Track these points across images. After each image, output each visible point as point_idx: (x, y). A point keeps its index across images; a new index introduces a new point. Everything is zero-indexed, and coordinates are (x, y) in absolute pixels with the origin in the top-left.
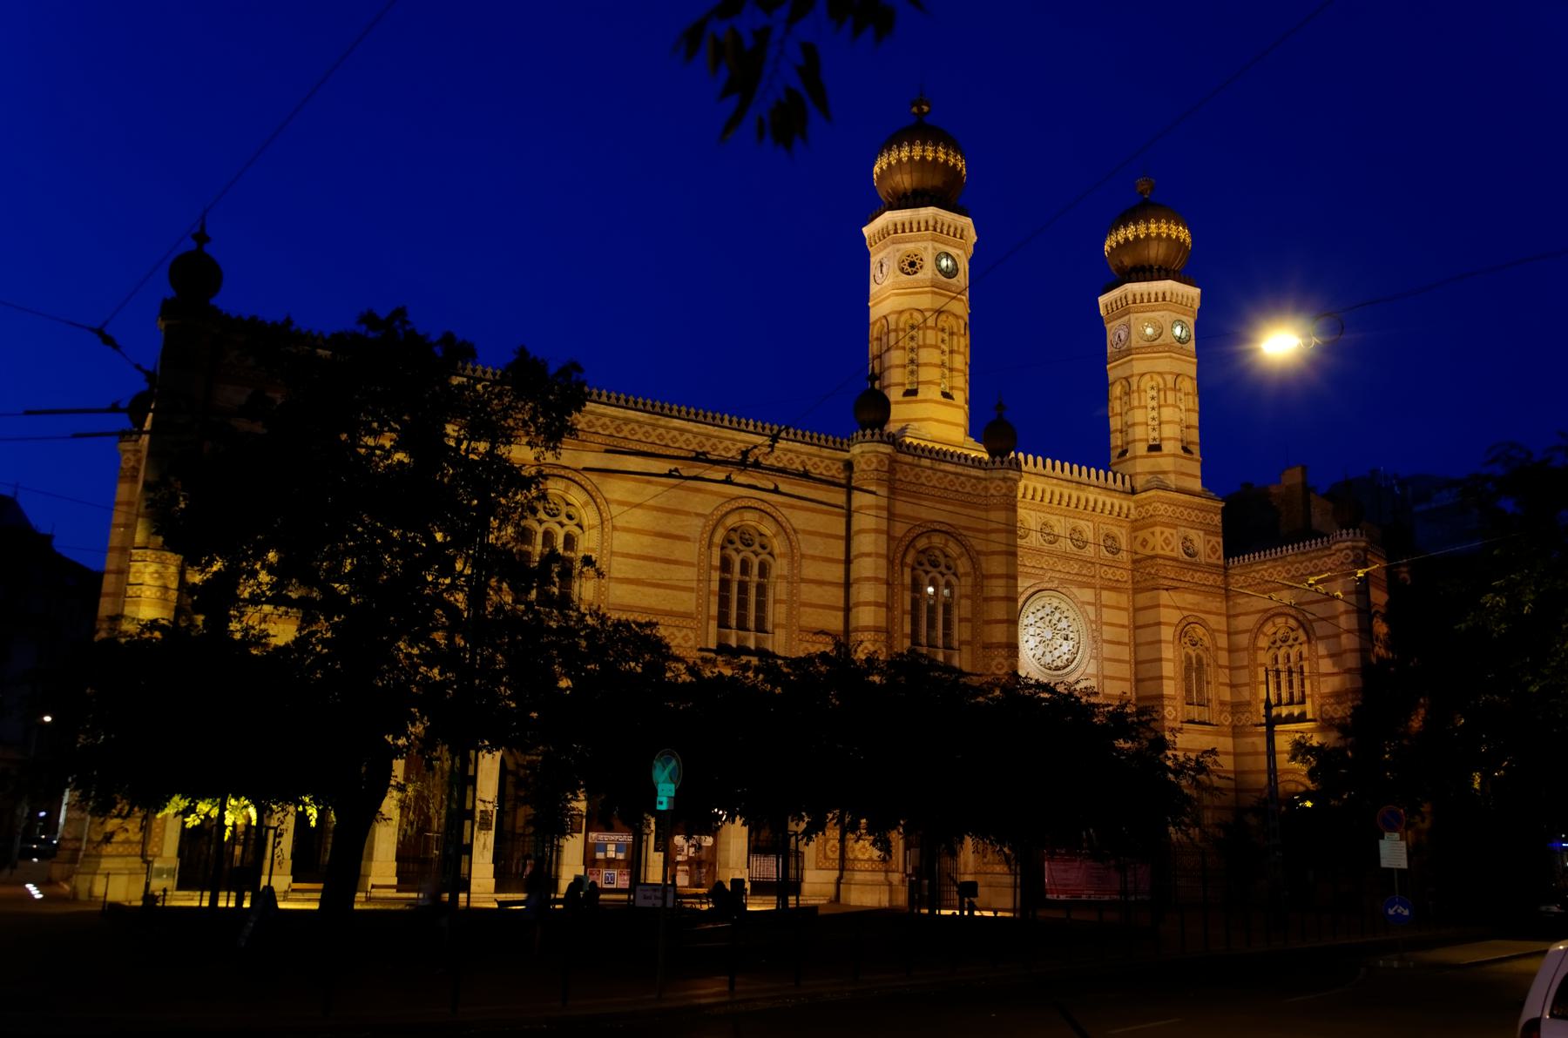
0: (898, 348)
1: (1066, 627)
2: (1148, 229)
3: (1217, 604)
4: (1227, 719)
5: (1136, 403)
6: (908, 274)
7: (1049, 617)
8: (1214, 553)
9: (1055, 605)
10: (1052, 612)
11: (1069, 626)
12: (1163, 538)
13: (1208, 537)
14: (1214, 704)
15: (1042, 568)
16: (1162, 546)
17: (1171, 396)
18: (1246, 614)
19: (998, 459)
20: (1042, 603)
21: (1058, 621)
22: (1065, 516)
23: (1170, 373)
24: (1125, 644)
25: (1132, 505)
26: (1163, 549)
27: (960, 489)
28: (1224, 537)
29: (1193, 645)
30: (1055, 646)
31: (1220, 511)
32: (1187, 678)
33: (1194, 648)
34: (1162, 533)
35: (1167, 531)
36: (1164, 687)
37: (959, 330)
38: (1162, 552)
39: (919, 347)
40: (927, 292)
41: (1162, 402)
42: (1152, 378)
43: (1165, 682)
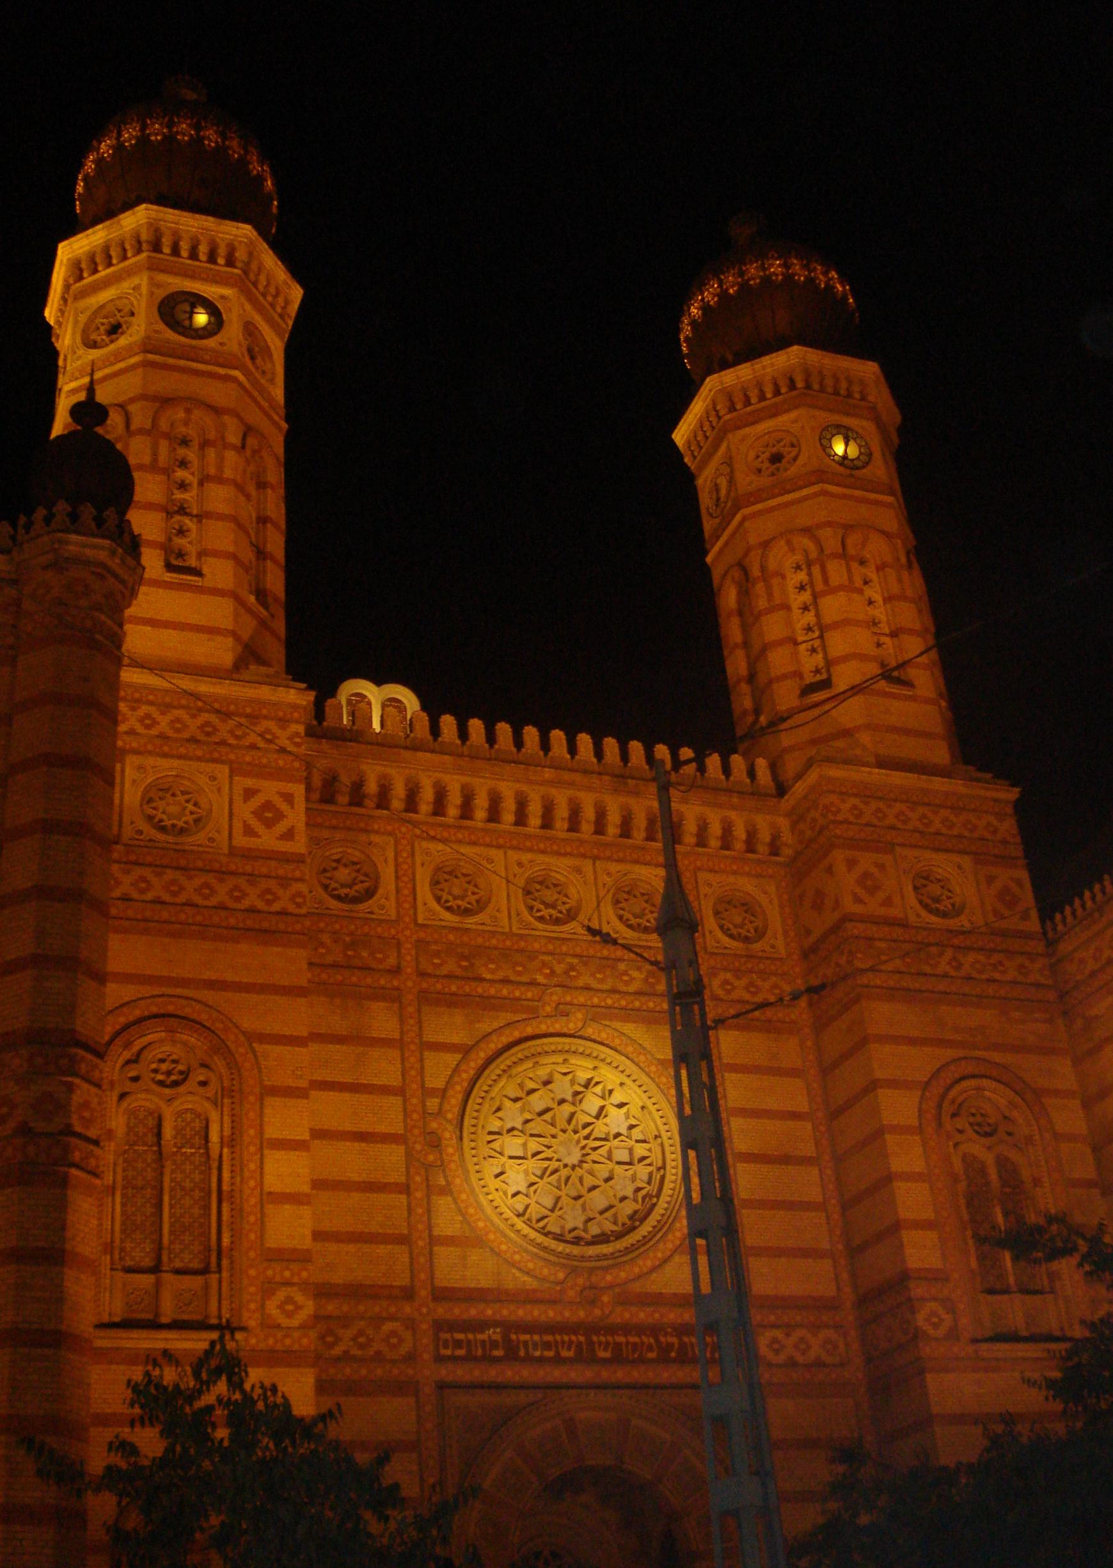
1: (624, 1131)
2: (741, 274)
7: (567, 1109)
9: (583, 1076)
10: (577, 1093)
11: (631, 1127)
15: (533, 983)
16: (855, 895)
17: (837, 572)
20: (543, 1073)
21: (597, 1117)
22: (595, 858)
23: (829, 524)
24: (806, 1161)
25: (784, 823)
28: (1031, 868)
29: (987, 1135)
30: (589, 1181)
31: (1009, 810)
33: (983, 1140)
34: (851, 864)
35: (866, 861)
36: (909, 1251)
38: (858, 909)
40: (133, 367)
41: (820, 586)
42: (789, 542)
43: (907, 1236)
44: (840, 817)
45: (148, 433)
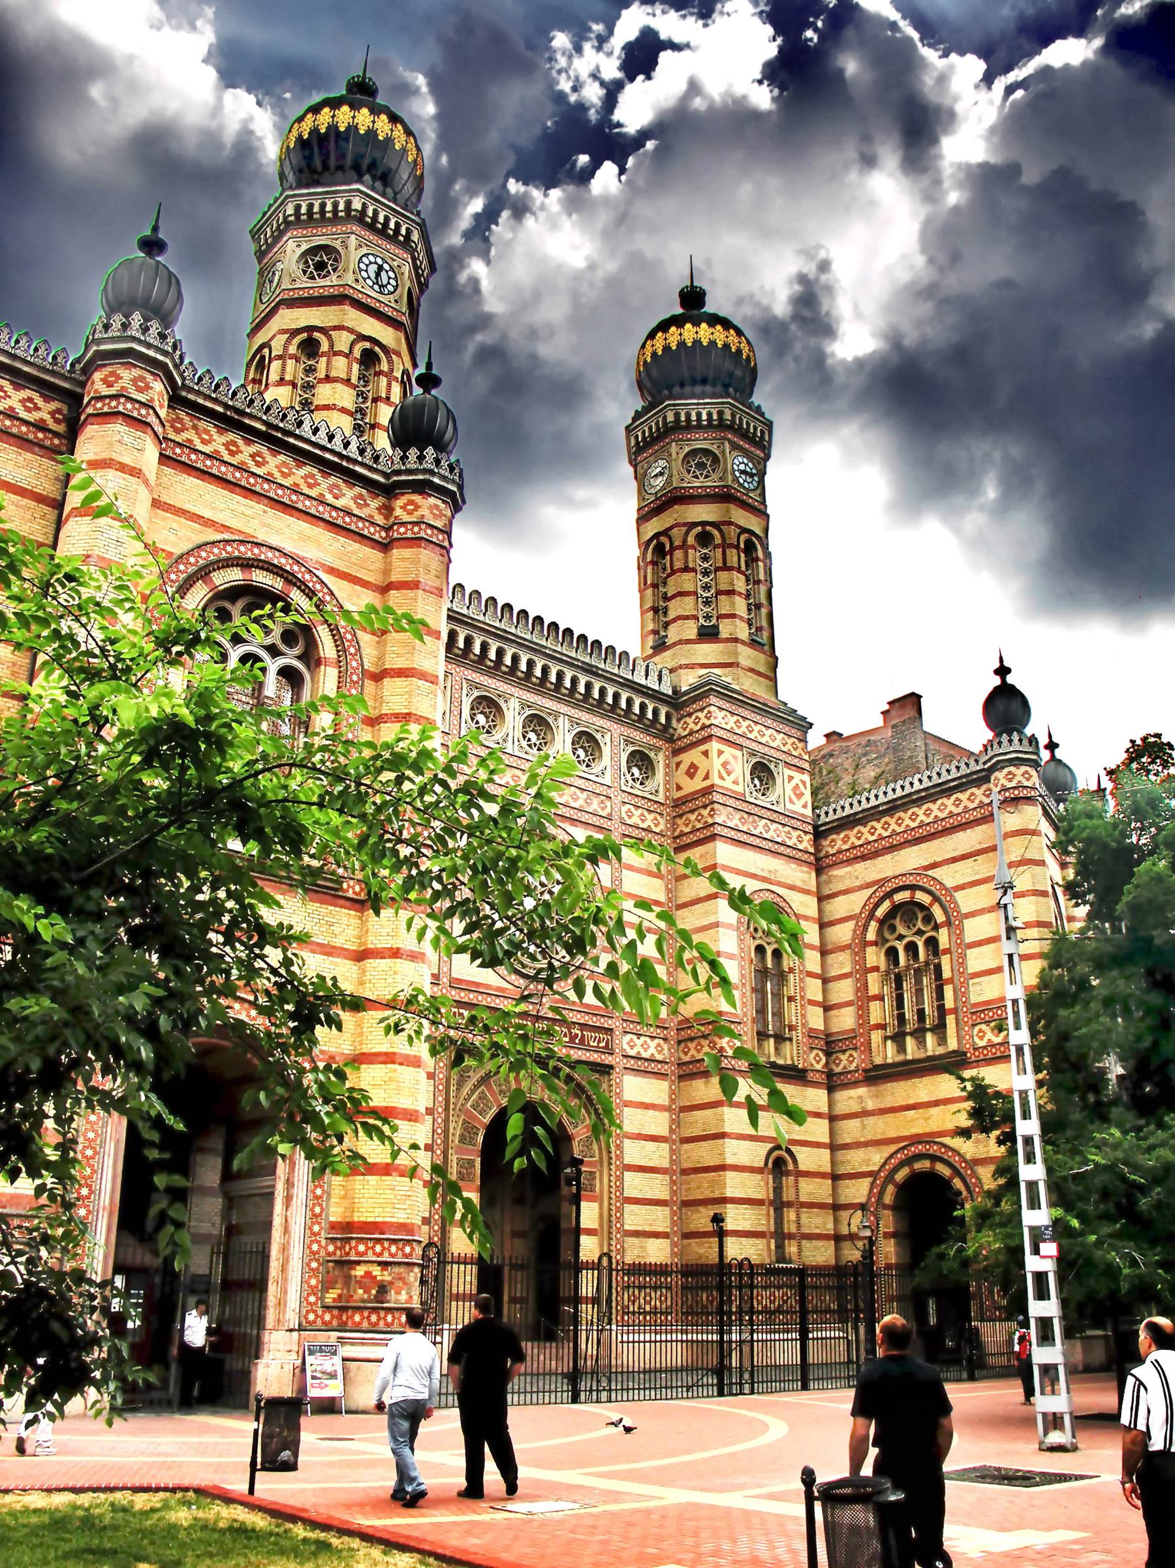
0: (281, 382)
3: (804, 876)
4: (816, 1061)
5: (678, 565)
6: (313, 278)
8: (800, 796)
12: (723, 758)
13: (787, 772)
14: (798, 1035)
18: (846, 892)
19: (413, 453)
23: (730, 523)
26: (721, 777)
27: (329, 498)
32: (760, 991)
34: (720, 753)
35: (729, 751)
37: (392, 370)
39: (320, 381)
44: (716, 722)
45: (347, 356)
